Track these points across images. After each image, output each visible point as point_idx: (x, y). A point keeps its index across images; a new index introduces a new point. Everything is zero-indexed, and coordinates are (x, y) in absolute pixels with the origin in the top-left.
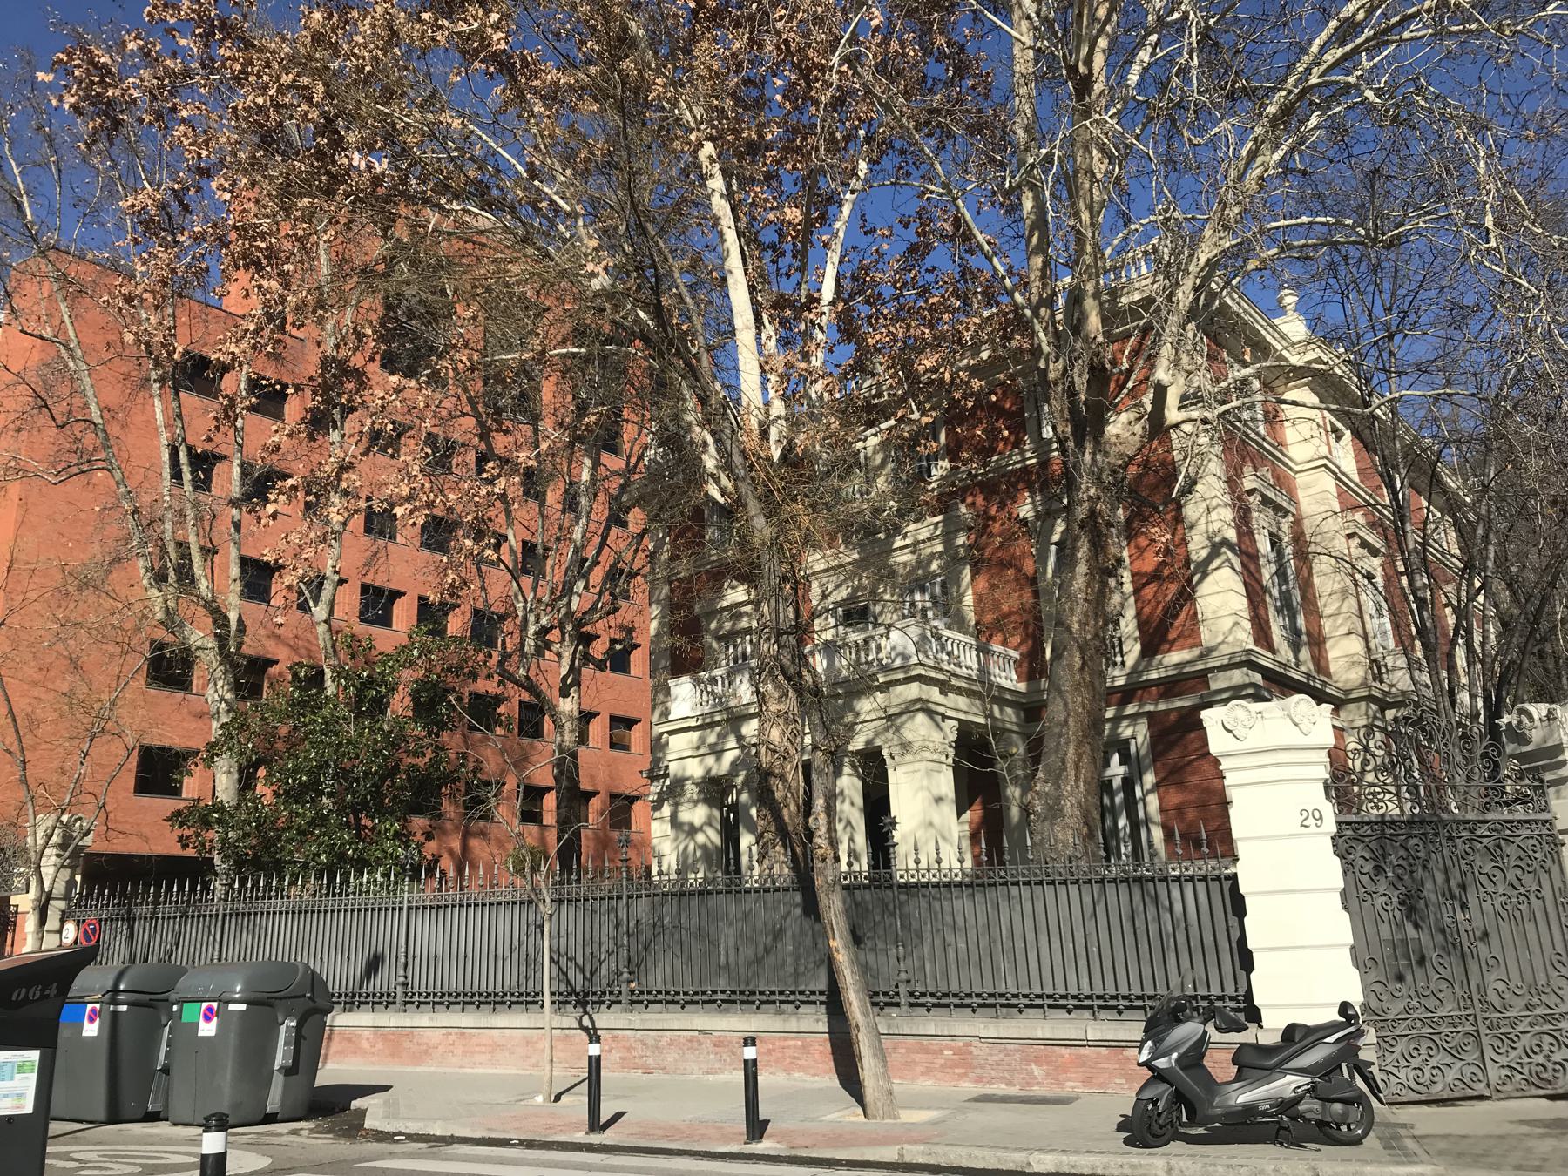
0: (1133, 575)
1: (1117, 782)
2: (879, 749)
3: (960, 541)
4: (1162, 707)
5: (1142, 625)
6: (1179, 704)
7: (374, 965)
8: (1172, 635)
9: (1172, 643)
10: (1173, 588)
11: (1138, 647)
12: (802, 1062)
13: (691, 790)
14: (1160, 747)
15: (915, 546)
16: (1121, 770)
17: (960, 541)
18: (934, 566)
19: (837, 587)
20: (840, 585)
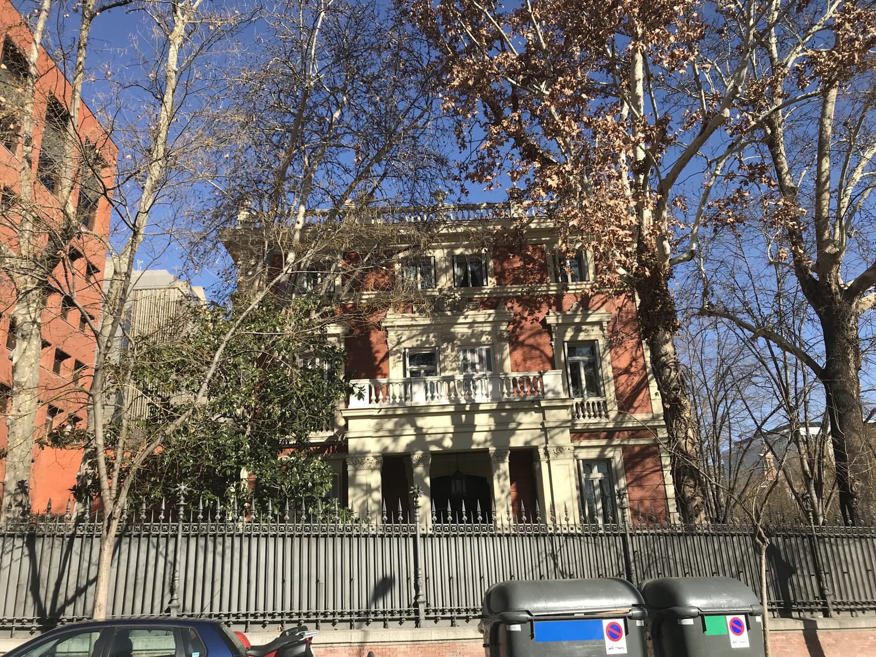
0: (613, 368)
1: (596, 483)
2: (536, 448)
3: (503, 328)
4: (632, 442)
5: (618, 396)
6: (642, 442)
7: (384, 586)
8: (636, 404)
9: (636, 408)
10: (637, 379)
11: (616, 408)
12: (788, 650)
13: (371, 460)
14: (629, 465)
15: (471, 325)
16: (600, 475)
17: (503, 328)
18: (484, 338)
19: (409, 338)
20: (412, 338)
